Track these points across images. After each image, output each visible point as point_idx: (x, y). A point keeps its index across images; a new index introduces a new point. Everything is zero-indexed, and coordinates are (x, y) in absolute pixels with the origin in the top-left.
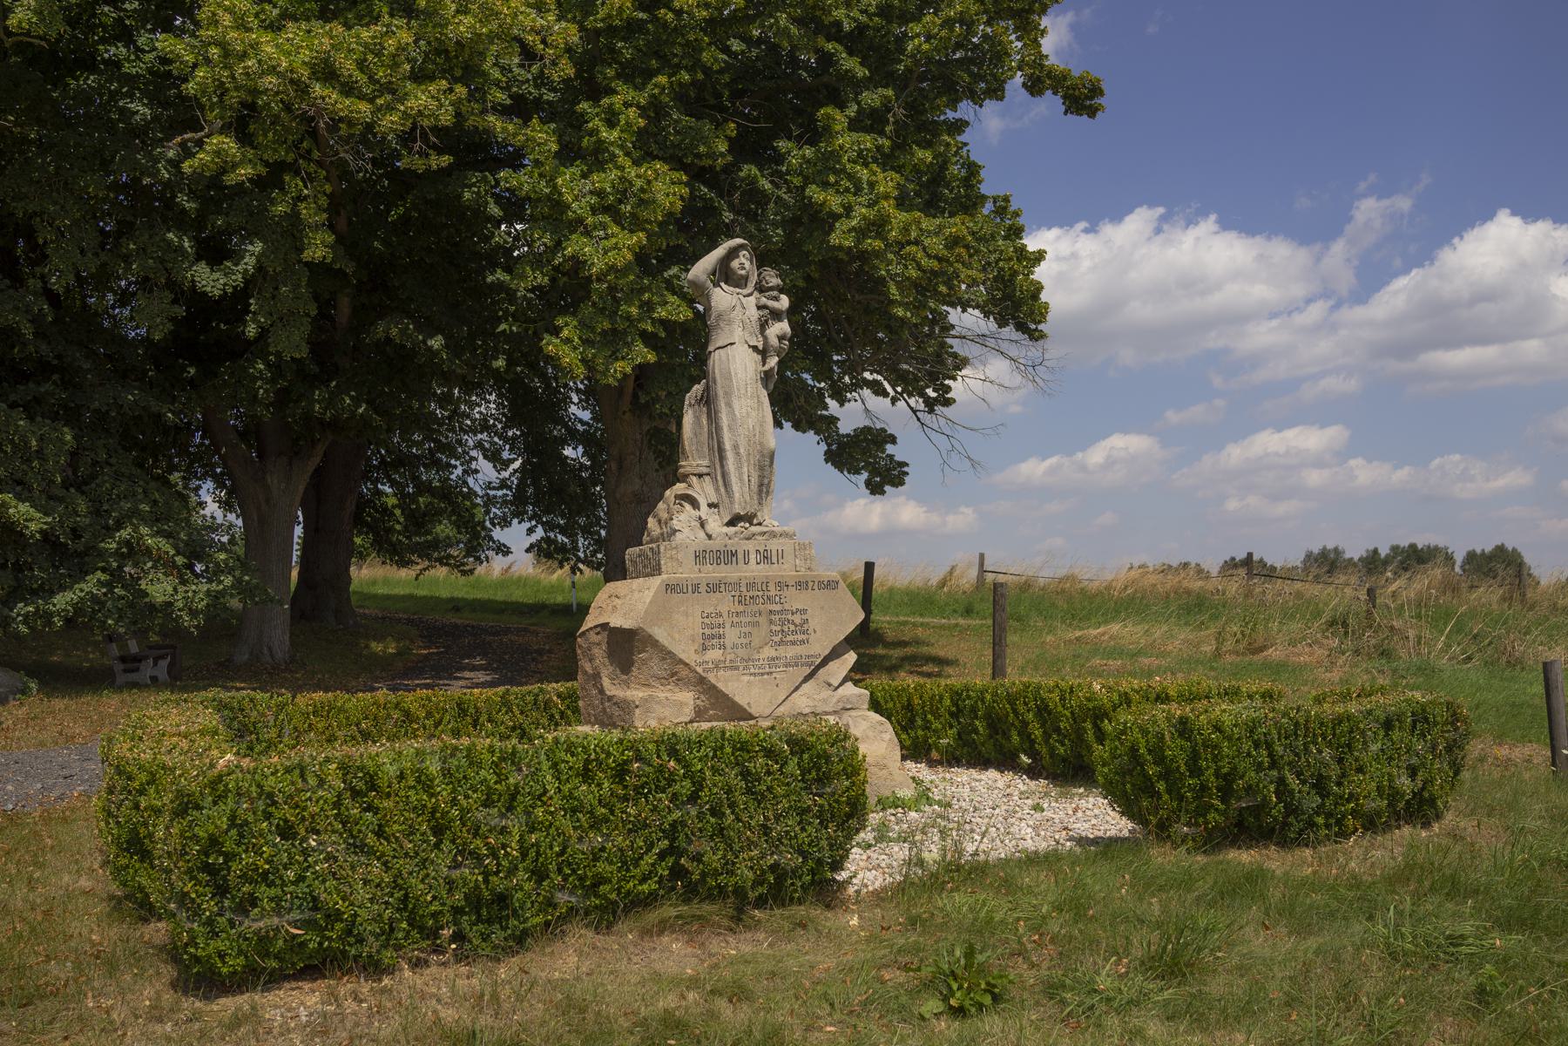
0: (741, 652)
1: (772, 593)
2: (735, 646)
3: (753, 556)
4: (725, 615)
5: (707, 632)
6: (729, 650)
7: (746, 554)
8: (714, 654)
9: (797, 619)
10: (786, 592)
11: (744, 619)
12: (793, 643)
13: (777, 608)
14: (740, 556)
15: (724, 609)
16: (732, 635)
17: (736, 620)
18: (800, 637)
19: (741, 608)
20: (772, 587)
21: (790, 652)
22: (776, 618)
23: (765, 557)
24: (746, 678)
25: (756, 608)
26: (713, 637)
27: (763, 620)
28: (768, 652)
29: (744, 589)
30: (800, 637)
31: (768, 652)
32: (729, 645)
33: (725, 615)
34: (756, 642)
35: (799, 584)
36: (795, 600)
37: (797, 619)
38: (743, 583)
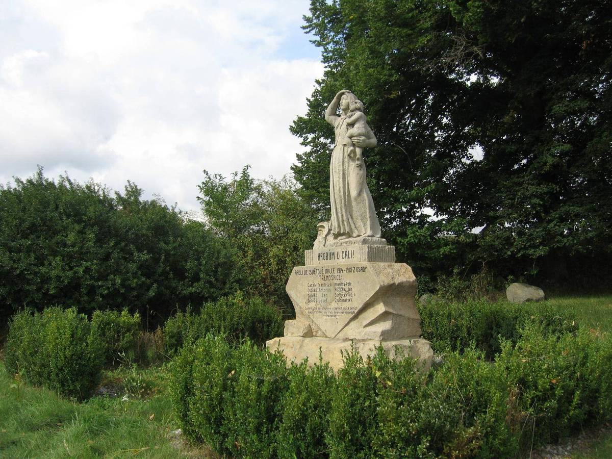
0: (323, 304)
1: (336, 274)
2: (321, 301)
3: (341, 255)
4: (317, 285)
5: (310, 293)
6: (318, 303)
7: (338, 254)
8: (312, 305)
9: (347, 288)
10: (342, 274)
11: (325, 288)
12: (345, 301)
13: (338, 282)
14: (336, 255)
15: (316, 282)
16: (319, 295)
17: (321, 288)
18: (348, 298)
19: (323, 282)
20: (336, 271)
21: (345, 305)
22: (337, 287)
23: (346, 254)
24: (325, 317)
25: (329, 282)
26: (312, 296)
27: (332, 288)
28: (334, 305)
29: (324, 272)
30: (348, 298)
31: (334, 305)
32: (318, 300)
33: (317, 285)
34: (329, 300)
35: (347, 269)
36: (346, 278)
37: (347, 288)
38: (324, 269)
